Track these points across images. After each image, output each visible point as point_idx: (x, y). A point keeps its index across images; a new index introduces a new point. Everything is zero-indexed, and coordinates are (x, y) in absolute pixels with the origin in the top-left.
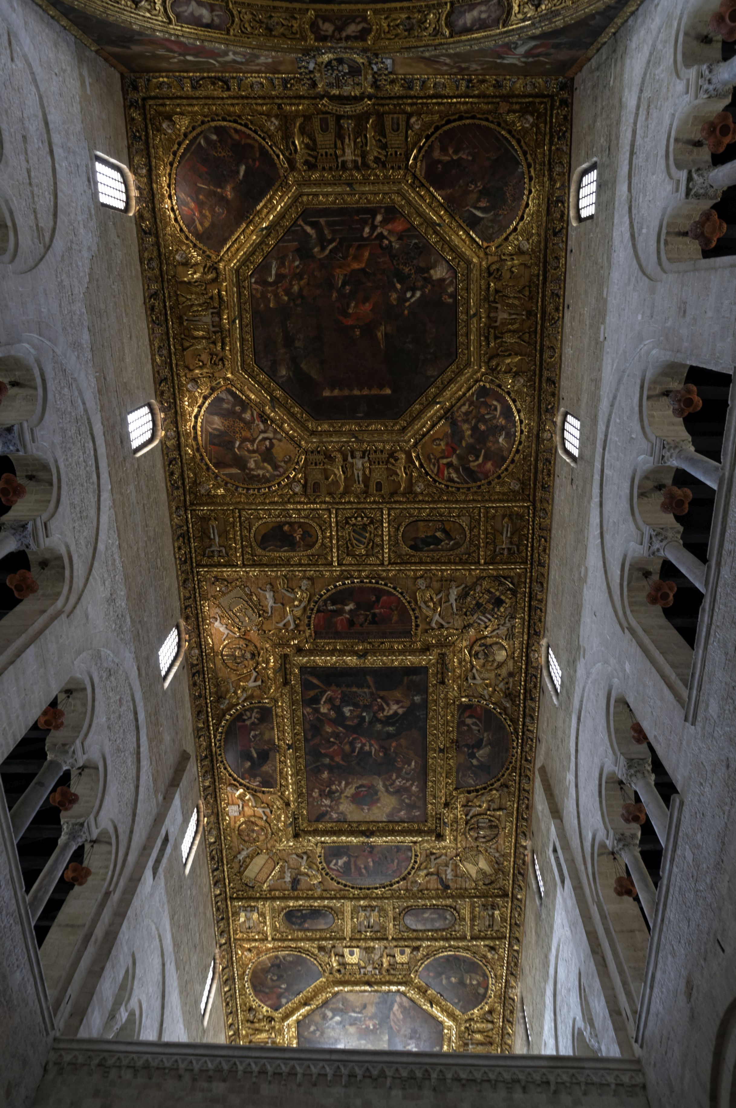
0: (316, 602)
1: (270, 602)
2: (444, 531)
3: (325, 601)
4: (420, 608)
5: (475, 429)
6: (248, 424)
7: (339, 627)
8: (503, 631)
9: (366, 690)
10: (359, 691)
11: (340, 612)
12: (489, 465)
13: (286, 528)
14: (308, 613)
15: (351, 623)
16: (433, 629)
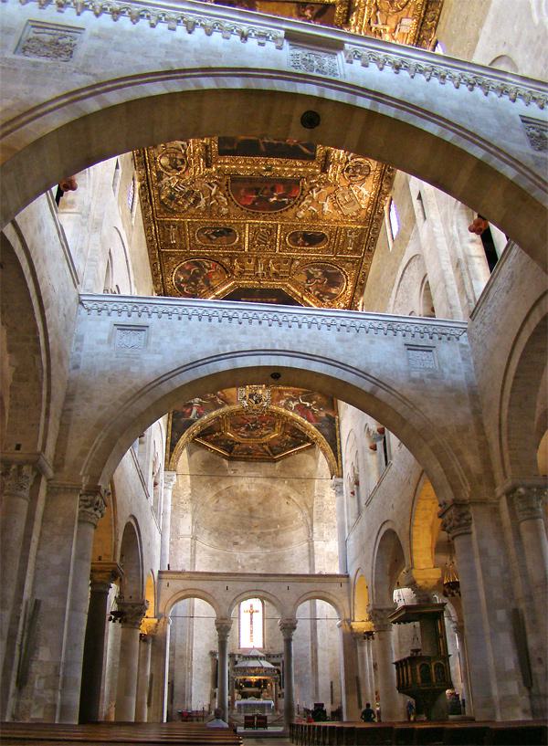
0: (295, 204)
1: (326, 205)
2: (211, 239)
3: (289, 203)
4: (225, 196)
5: (197, 282)
6: (317, 289)
7: (282, 187)
8: (166, 179)
9: (267, 141)
10: (272, 141)
11: (279, 197)
12: (187, 268)
13: (307, 244)
14: (302, 198)
15: (273, 190)
16: (215, 183)
